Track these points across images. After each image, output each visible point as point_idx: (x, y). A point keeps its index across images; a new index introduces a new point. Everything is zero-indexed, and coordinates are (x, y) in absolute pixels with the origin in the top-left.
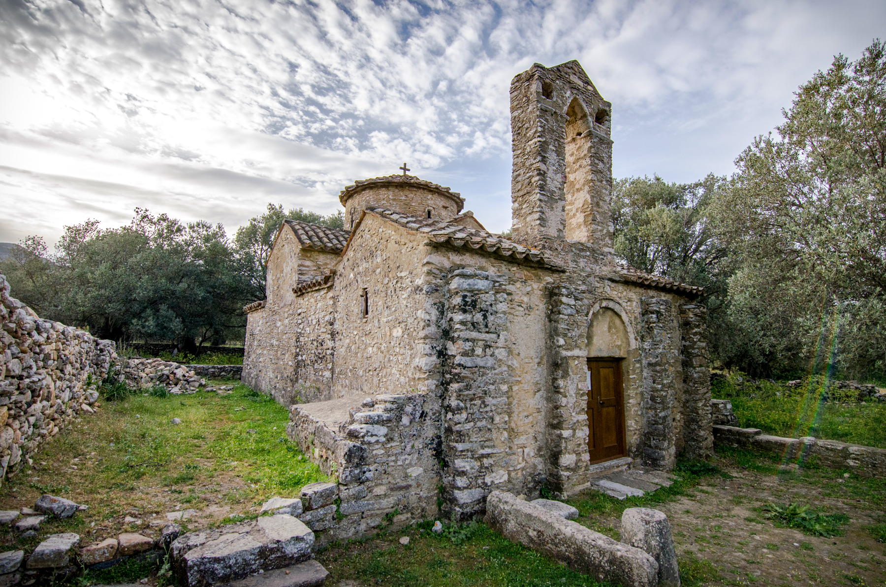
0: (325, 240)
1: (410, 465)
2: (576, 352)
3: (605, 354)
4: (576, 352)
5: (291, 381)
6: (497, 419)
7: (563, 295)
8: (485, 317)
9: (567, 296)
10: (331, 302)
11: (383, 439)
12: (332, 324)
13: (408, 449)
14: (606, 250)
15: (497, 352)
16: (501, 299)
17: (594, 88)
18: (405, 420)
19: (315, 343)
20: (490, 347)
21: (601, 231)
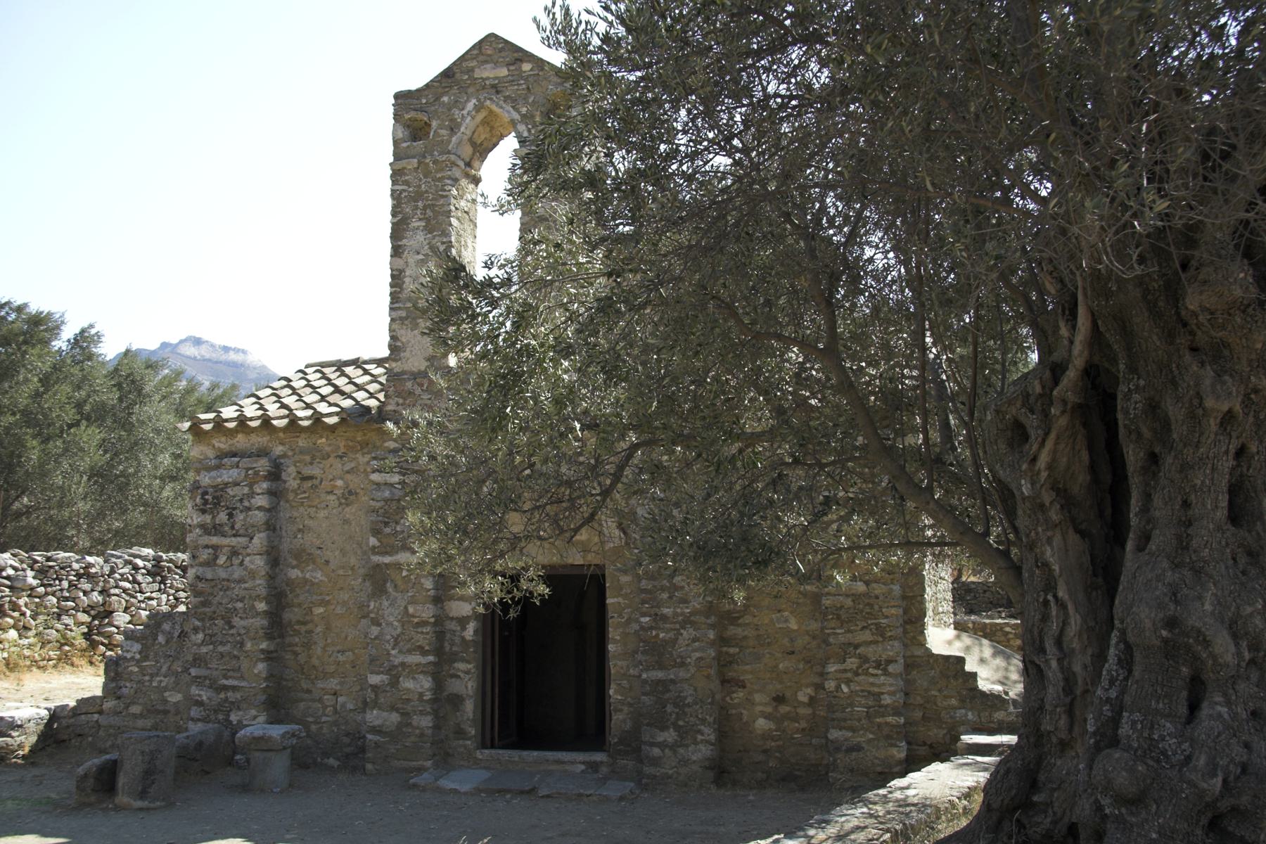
8: (230, 515)
11: (138, 656)
13: (164, 669)
15: (248, 559)
16: (259, 491)
18: (161, 639)
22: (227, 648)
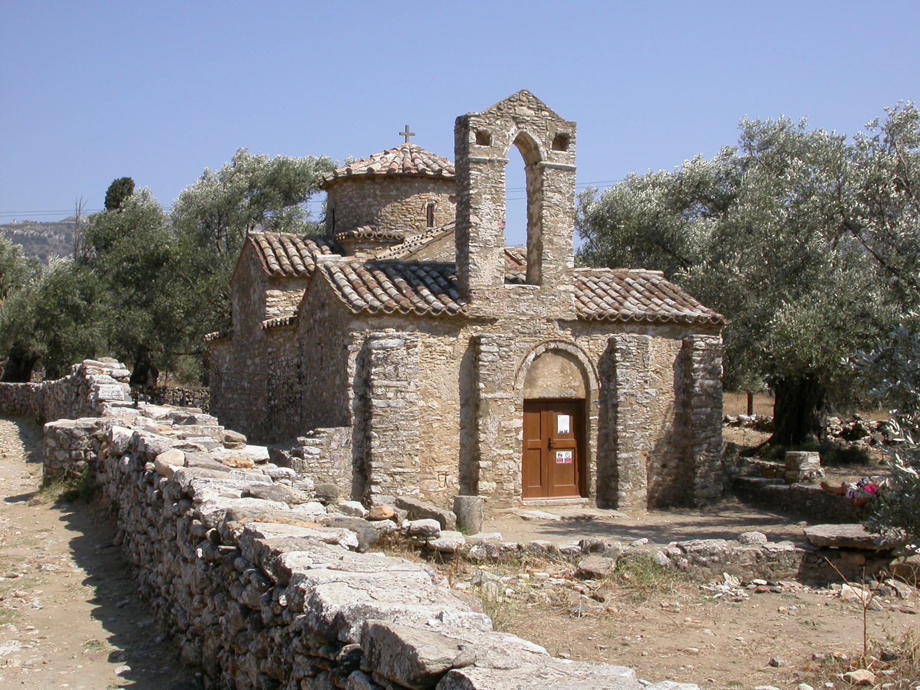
0: (297, 260)
1: (339, 476)
2: (499, 394)
3: (553, 393)
4: (499, 394)
6: (409, 447)
8: (396, 369)
9: (486, 344)
10: (297, 345)
12: (299, 367)
13: (337, 464)
14: (562, 288)
15: (407, 396)
17: (550, 111)
18: (334, 445)
19: (286, 387)
22: (396, 449)
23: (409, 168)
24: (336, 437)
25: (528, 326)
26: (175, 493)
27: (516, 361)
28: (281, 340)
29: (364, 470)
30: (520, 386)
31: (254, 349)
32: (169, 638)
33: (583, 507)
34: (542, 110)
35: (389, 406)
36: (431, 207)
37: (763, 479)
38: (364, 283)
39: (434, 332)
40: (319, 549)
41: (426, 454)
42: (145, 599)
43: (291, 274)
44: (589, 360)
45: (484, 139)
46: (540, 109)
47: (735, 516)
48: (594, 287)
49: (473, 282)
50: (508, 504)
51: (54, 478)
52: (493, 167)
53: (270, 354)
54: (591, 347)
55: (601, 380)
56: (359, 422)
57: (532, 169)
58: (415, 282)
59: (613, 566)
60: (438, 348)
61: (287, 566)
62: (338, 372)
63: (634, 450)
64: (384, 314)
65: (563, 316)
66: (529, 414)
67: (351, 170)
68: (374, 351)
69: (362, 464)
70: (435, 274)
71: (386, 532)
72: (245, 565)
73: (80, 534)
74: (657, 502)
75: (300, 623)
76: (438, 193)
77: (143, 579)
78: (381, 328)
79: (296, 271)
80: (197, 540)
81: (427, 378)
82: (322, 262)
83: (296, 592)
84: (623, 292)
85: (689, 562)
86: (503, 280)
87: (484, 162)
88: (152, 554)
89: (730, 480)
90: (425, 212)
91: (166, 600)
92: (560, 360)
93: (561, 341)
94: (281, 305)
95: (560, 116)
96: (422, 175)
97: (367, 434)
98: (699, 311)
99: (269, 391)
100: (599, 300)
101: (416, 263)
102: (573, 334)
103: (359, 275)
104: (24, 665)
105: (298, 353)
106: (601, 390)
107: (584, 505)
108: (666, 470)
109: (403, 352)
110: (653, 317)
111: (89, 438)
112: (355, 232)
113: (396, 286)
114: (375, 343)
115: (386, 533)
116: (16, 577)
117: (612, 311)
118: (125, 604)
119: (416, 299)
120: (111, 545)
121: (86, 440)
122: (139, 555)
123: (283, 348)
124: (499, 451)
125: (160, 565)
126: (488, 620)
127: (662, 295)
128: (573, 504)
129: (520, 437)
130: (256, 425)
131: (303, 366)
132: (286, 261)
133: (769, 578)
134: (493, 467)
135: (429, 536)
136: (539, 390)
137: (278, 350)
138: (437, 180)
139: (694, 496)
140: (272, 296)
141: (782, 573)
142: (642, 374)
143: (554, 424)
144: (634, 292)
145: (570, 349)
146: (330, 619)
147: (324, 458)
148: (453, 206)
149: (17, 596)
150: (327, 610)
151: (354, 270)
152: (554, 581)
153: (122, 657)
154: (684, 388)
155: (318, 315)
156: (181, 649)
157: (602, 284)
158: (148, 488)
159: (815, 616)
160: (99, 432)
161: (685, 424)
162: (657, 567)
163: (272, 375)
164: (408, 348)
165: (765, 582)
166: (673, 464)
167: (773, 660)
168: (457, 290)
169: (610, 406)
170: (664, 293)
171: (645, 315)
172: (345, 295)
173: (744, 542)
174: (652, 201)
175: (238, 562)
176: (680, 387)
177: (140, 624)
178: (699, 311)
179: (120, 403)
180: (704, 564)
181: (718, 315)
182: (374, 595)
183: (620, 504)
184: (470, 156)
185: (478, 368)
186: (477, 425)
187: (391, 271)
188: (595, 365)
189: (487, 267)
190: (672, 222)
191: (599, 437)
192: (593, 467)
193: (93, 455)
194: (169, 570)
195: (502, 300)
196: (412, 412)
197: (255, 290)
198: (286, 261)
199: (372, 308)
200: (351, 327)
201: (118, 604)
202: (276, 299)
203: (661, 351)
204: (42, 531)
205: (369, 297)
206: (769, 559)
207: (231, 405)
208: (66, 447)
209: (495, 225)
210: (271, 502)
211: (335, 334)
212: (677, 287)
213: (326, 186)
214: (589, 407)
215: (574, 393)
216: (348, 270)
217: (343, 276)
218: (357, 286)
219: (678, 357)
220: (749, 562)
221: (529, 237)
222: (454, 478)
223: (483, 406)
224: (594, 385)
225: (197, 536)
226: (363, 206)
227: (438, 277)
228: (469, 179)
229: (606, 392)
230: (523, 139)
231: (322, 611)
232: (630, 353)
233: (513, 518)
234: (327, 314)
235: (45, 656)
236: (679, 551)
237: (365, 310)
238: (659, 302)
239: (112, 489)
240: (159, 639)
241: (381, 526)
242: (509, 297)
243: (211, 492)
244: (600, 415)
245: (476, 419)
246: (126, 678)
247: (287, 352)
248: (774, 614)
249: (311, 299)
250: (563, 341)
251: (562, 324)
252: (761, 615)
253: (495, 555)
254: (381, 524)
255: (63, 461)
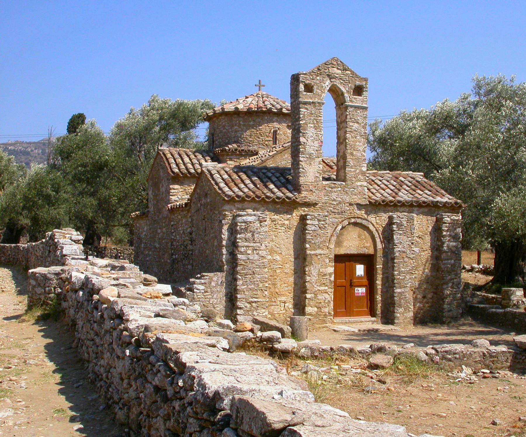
0: (190, 166)
1: (216, 304)
2: (318, 252)
3: (353, 251)
4: (318, 252)
5: (170, 273)
6: (261, 285)
7: (308, 220)
8: (253, 235)
9: (310, 219)
10: (190, 220)
12: (191, 234)
13: (215, 296)
14: (359, 184)
17: (351, 71)
18: (213, 284)
19: (183, 247)
20: (256, 250)
21: (355, 171)
22: (253, 286)
23: (261, 107)
24: (215, 279)
25: (337, 208)
26: (112, 315)
27: (330, 230)
28: (180, 217)
29: (233, 300)
30: (332, 246)
31: (162, 223)
32: (108, 407)
33: (373, 324)
34: (346, 70)
35: (248, 259)
36: (275, 132)
37: (487, 306)
38: (233, 180)
39: (277, 212)
40: (204, 350)
41: (272, 290)
42: (93, 382)
43: (186, 175)
44: (376, 230)
45: (309, 88)
46: (345, 69)
47: (469, 329)
48: (380, 183)
49: (302, 180)
50: (324, 322)
51: (35, 305)
52: (315, 107)
53: (172, 226)
54: (377, 221)
55: (384, 242)
56: (230, 269)
57: (340, 108)
58: (265, 180)
59: (392, 361)
60: (280, 222)
61: (184, 361)
62: (216, 237)
63: (405, 287)
64: (246, 200)
65: (359, 202)
66: (338, 264)
67: (224, 109)
68: (239, 224)
69: (232, 296)
70: (278, 175)
71: (246, 340)
72: (156, 361)
73: (51, 341)
74: (420, 320)
75: (191, 397)
76: (280, 123)
77: (91, 369)
78: (243, 209)
79: (189, 173)
80: (126, 344)
81: (272, 241)
82: (206, 167)
83: (189, 378)
84: (398, 186)
85: (440, 359)
86: (321, 179)
87: (309, 103)
88: (97, 353)
89: (466, 306)
90: (271, 135)
91: (106, 383)
92: (358, 230)
93: (358, 218)
94: (179, 195)
95: (358, 74)
96: (269, 112)
97: (234, 277)
98: (447, 198)
99: (172, 249)
100: (383, 192)
101: (266, 168)
102: (366, 213)
103: (229, 176)
104: (15, 424)
105: (190, 225)
106: (384, 249)
107: (373, 322)
108: (425, 300)
109: (257, 224)
110: (417, 202)
111: (57, 280)
112: (227, 148)
113: (253, 182)
114: (239, 219)
115: (246, 340)
116: (10, 368)
117: (391, 198)
118: (79, 385)
119: (266, 191)
120: (71, 348)
121: (55, 281)
122: (89, 354)
123: (181, 222)
124: (319, 288)
125: (102, 361)
126: (311, 396)
127: (423, 188)
128: (366, 322)
129: (332, 279)
130: (163, 271)
131: (194, 233)
132: (182, 167)
133: (491, 369)
134: (315, 298)
135: (274, 342)
136: (344, 249)
137: (178, 223)
138: (279, 115)
139: (443, 317)
140: (174, 189)
141: (499, 366)
142: (410, 239)
143: (353, 271)
144: (405, 186)
145: (364, 222)
146: (211, 395)
147: (207, 292)
148: (289, 132)
149: (11, 380)
150: (209, 389)
151: (226, 172)
152: (354, 371)
153: (78, 419)
154: (437, 247)
155: (203, 201)
156: (116, 414)
157: (384, 181)
158: (95, 311)
159: (520, 393)
160: (63, 275)
161: (438, 271)
162: (419, 361)
163: (173, 239)
164: (261, 222)
165: (488, 371)
166: (430, 296)
167: (494, 421)
168: (292, 185)
169: (389, 259)
170: (424, 187)
171: (412, 201)
172: (220, 188)
173: (475, 346)
174: (417, 128)
175: (152, 358)
176: (434, 247)
177: (90, 398)
178: (447, 198)
179: (76, 257)
180: (450, 360)
181: (459, 201)
182: (238, 379)
183: (396, 321)
184: (300, 100)
185: (305, 235)
186: (305, 271)
187: (250, 173)
188: (380, 233)
189: (311, 170)
190: (429, 141)
191: (382, 279)
192: (379, 298)
193: (60, 290)
194: (108, 364)
195: (321, 191)
196: (263, 263)
197: (163, 185)
198: (182, 167)
199: (238, 196)
200: (225, 208)
201: (75, 385)
202: (176, 191)
203: (422, 223)
204: (27, 338)
205: (236, 189)
206: (491, 356)
207: (148, 259)
208: (42, 285)
209: (316, 144)
210: (173, 320)
211: (214, 213)
212: (432, 183)
213: (208, 118)
214: (376, 260)
215: (367, 250)
216: (222, 172)
217: (219, 176)
218: (228, 182)
219: (433, 227)
220: (478, 359)
221: (338, 151)
222: (290, 305)
223: (308, 259)
224: (379, 246)
225: (125, 342)
226: (232, 132)
227: (280, 177)
228: (300, 114)
229: (387, 250)
230: (334, 89)
231: (206, 390)
232: (402, 225)
233: (328, 330)
234: (209, 200)
235: (28, 418)
236: (433, 352)
237: (233, 197)
238: (421, 193)
239: (72, 312)
240: (101, 407)
241: (243, 335)
242: (325, 189)
243: (135, 314)
244: (383, 265)
245: (304, 267)
246: (80, 432)
247: (183, 225)
248: (494, 391)
249: (199, 191)
250: (359, 218)
251: (359, 207)
252: (486, 392)
253: (316, 354)
254: (244, 334)
255: (40, 294)
